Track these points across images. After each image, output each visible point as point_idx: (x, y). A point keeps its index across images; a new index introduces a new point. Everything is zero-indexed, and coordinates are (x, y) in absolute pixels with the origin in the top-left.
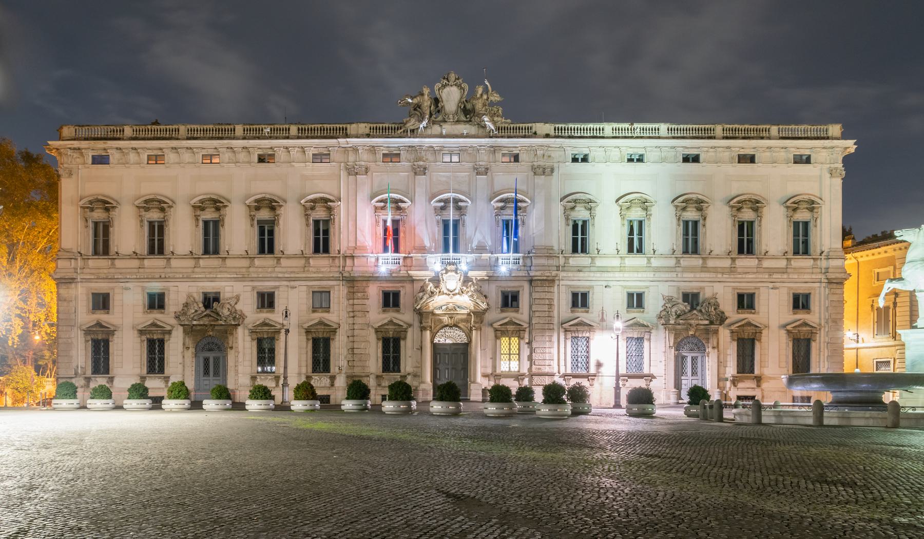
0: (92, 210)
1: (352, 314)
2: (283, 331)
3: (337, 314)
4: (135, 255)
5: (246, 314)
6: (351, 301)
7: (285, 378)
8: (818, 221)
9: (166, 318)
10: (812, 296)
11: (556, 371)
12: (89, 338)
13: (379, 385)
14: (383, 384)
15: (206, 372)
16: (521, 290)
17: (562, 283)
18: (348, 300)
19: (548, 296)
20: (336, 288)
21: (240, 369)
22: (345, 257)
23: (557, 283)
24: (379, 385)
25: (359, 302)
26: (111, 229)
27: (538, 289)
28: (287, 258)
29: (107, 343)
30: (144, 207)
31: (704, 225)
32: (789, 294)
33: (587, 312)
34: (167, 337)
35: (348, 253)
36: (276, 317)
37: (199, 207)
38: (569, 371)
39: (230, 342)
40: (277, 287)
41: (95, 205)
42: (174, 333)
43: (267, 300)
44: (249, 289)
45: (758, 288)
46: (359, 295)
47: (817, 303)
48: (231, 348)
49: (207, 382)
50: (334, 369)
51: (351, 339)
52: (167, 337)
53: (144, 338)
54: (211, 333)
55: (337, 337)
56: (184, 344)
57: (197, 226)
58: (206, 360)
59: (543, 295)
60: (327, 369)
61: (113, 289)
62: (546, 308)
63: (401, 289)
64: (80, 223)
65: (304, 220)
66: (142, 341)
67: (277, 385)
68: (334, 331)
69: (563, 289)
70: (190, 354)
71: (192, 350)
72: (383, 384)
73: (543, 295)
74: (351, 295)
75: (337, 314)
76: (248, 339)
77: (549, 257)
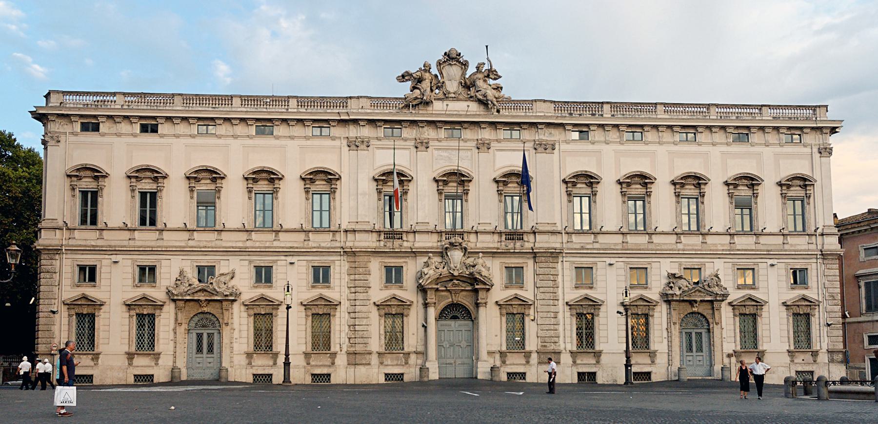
0: (79, 178)
1: (353, 290)
2: (283, 308)
3: (338, 289)
4: (126, 228)
5: (242, 289)
6: (352, 277)
7: (287, 355)
8: (812, 198)
9: (157, 293)
10: (809, 271)
11: (562, 347)
12: (73, 312)
13: (382, 363)
14: (386, 363)
15: (199, 350)
16: (524, 265)
17: (565, 259)
18: (349, 275)
19: (553, 272)
20: (337, 263)
21: (235, 346)
22: (346, 231)
23: (560, 259)
24: (382, 363)
25: (361, 277)
26: (100, 199)
27: (542, 265)
28: (286, 231)
29: (92, 317)
30: (137, 177)
31: (703, 203)
32: (786, 270)
33: (591, 288)
34: (157, 312)
35: (350, 227)
36: (275, 293)
37: (193, 177)
38: (575, 349)
39: (226, 318)
40: (275, 261)
41: (82, 174)
42: (165, 308)
43: (264, 275)
44: (246, 263)
45: (757, 264)
46: (361, 270)
47: (815, 279)
48: (227, 324)
49: (198, 360)
50: (334, 348)
51: (352, 315)
52: (157, 312)
53: (133, 313)
54: (205, 309)
55: (338, 314)
56: (176, 320)
57: (192, 198)
58: (200, 337)
59: (547, 271)
60: (328, 346)
61: (100, 260)
62: (551, 283)
63: (403, 265)
64: (68, 193)
65: (304, 195)
66: (131, 316)
67: (275, 364)
68: (334, 306)
69: (566, 265)
70: (181, 330)
71: (185, 326)
72: (386, 363)
73: (547, 271)
74: (353, 270)
75: (338, 289)
76: (245, 315)
77: (553, 233)
